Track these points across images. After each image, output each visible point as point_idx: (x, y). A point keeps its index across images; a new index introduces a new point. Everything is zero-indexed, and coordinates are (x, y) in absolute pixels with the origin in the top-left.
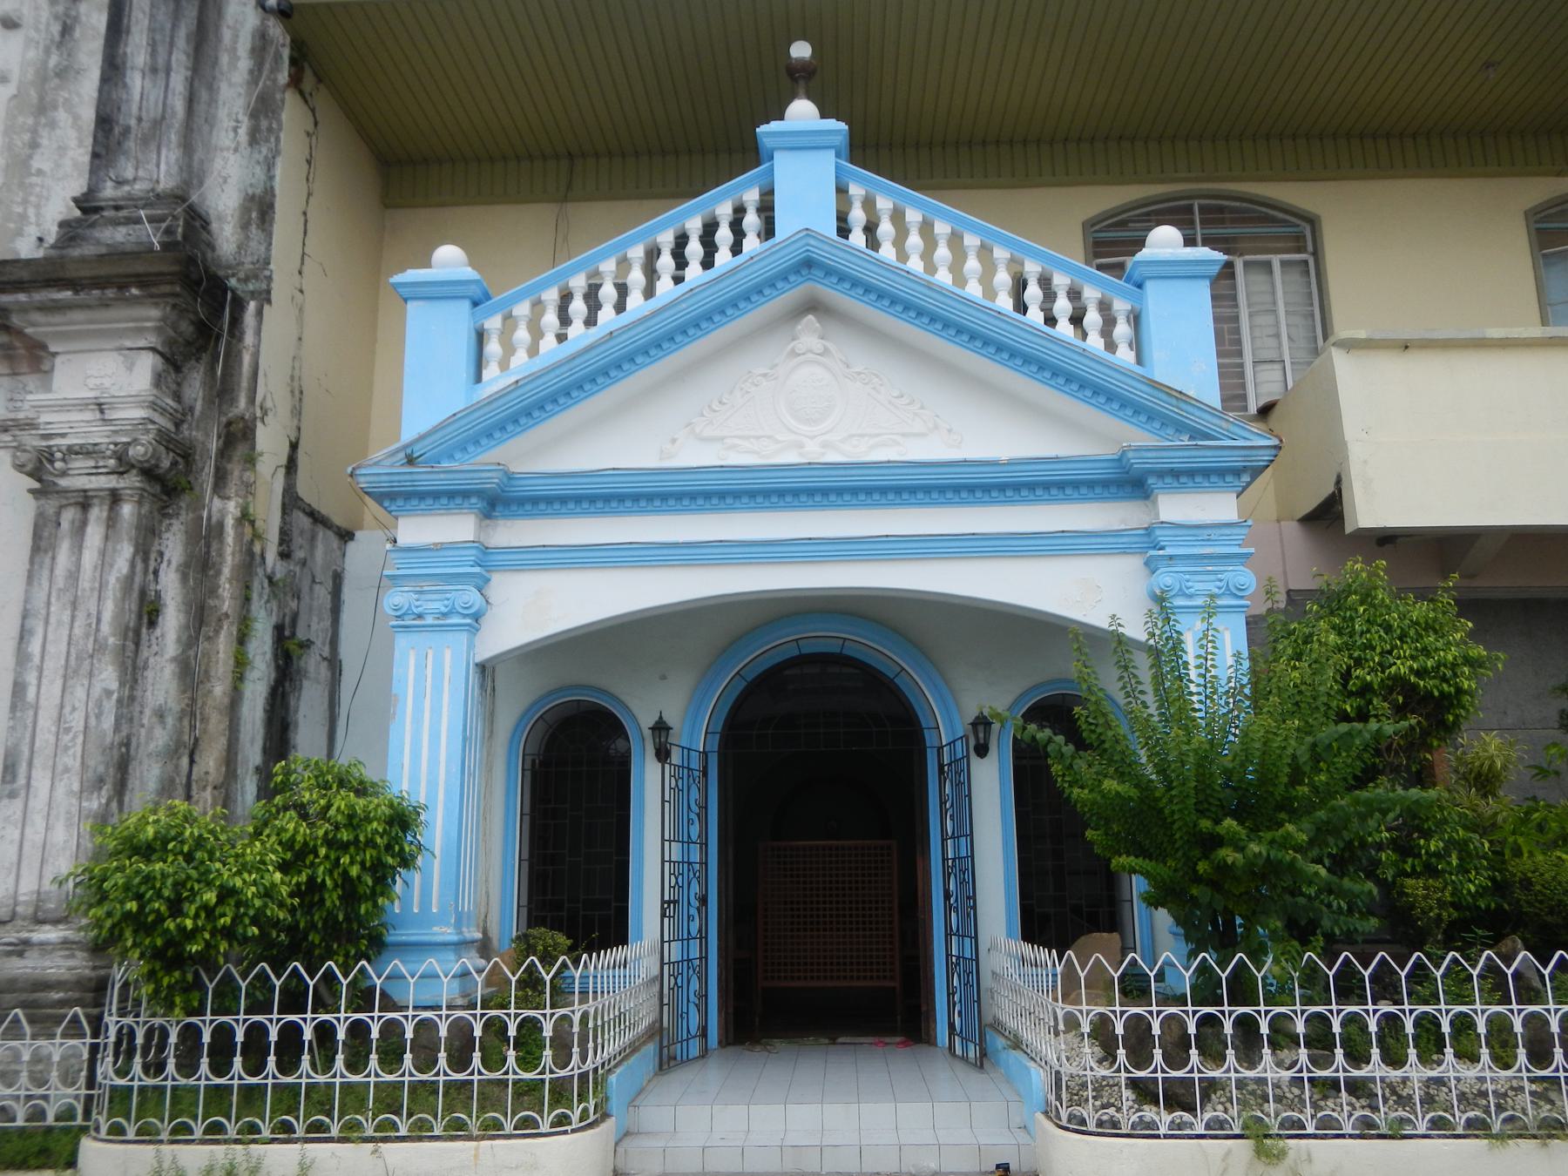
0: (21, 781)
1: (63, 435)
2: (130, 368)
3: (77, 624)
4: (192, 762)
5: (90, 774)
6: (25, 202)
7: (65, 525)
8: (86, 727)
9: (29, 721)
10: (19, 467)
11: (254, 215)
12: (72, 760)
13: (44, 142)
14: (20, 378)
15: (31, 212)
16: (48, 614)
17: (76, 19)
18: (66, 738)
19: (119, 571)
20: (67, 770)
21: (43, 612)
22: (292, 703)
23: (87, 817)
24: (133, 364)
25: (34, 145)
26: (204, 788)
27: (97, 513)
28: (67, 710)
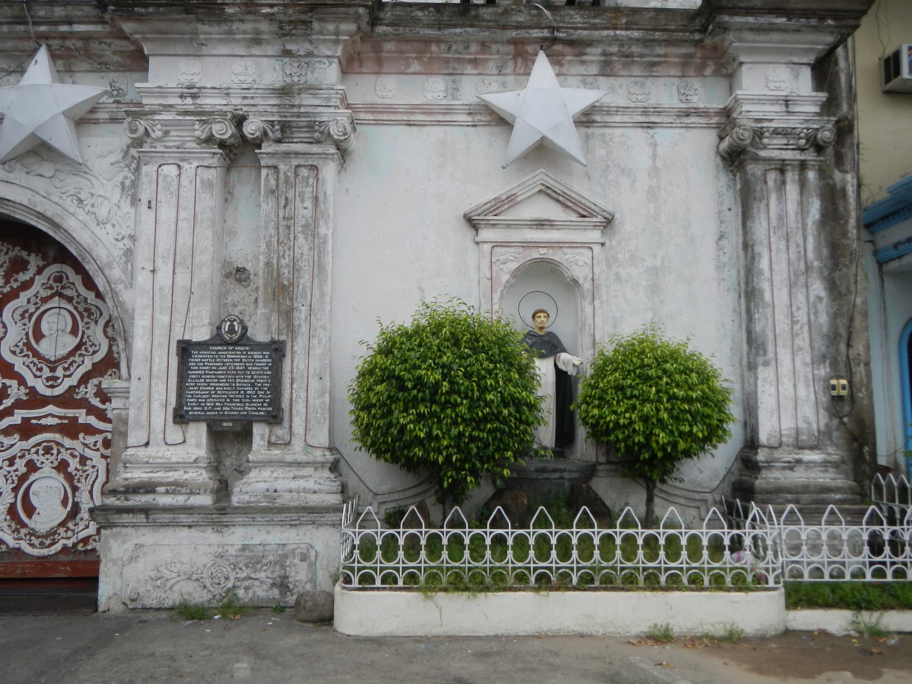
0: (771, 355)
3: (791, 251)
4: (849, 345)
5: (816, 352)
7: (771, 183)
8: (809, 321)
9: (769, 315)
12: (803, 341)
14: (685, 79)
16: (770, 243)
18: (796, 328)
19: (813, 216)
20: (800, 349)
21: (766, 242)
23: (819, 380)
26: (858, 364)
28: (794, 308)
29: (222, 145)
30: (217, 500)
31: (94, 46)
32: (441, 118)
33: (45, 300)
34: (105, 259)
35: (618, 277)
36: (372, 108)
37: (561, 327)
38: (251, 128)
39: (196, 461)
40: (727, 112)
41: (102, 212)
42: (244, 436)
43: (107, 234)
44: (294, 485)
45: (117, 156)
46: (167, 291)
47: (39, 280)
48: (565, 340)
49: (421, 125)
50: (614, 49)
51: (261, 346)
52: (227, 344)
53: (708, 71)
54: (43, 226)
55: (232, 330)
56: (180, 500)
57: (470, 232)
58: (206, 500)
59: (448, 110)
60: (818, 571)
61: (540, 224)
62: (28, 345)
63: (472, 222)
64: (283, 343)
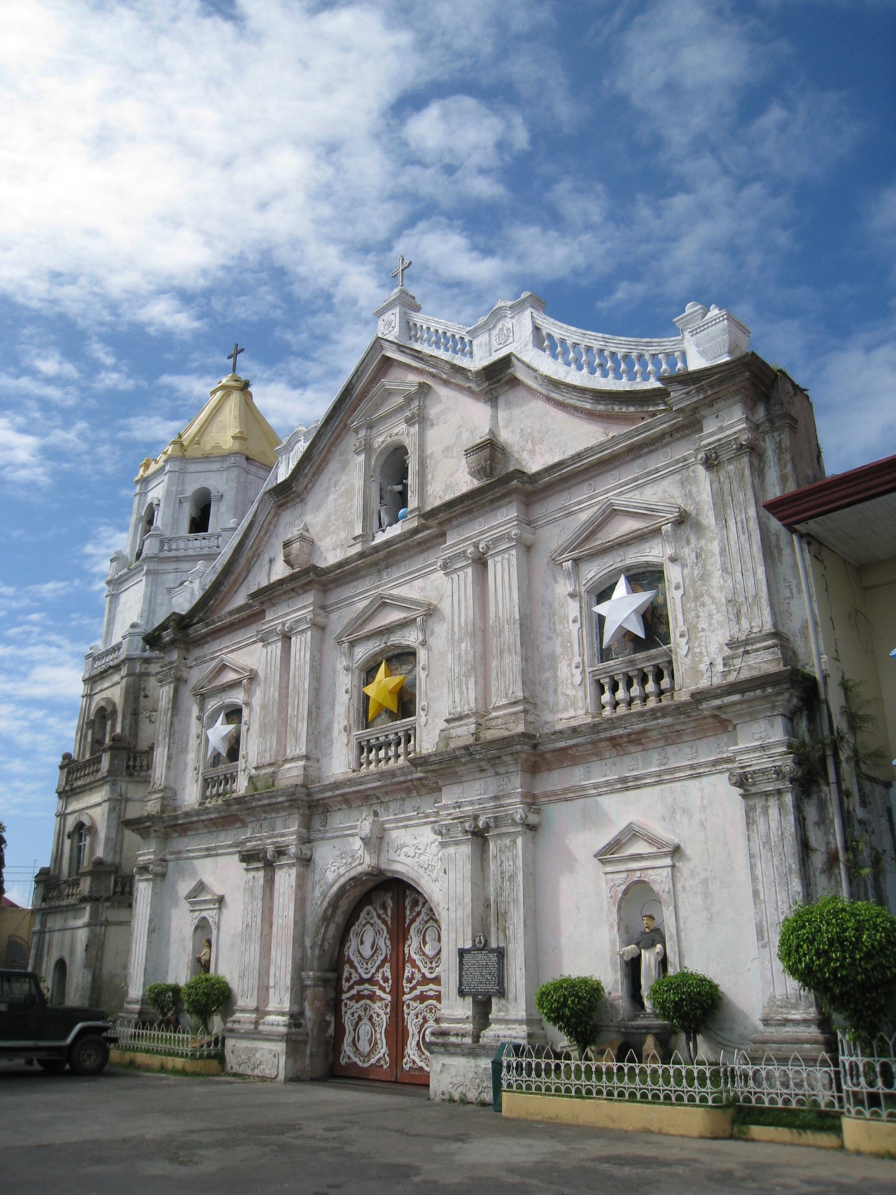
1: (750, 766)
2: (772, 726)
6: (700, 646)
10: (735, 784)
13: (701, 614)
15: (704, 650)
17: (701, 549)
22: (883, 885)
24: (773, 724)
25: (698, 617)
30: (474, 1042)
31: (424, 782)
32: (581, 793)
33: (426, 922)
35: (684, 888)
36: (546, 795)
39: (467, 1018)
44: (508, 1033)
46: (454, 920)
47: (424, 910)
50: (665, 730)
51: (492, 951)
52: (478, 950)
54: (413, 884)
55: (480, 942)
60: (786, 1102)
62: (420, 948)
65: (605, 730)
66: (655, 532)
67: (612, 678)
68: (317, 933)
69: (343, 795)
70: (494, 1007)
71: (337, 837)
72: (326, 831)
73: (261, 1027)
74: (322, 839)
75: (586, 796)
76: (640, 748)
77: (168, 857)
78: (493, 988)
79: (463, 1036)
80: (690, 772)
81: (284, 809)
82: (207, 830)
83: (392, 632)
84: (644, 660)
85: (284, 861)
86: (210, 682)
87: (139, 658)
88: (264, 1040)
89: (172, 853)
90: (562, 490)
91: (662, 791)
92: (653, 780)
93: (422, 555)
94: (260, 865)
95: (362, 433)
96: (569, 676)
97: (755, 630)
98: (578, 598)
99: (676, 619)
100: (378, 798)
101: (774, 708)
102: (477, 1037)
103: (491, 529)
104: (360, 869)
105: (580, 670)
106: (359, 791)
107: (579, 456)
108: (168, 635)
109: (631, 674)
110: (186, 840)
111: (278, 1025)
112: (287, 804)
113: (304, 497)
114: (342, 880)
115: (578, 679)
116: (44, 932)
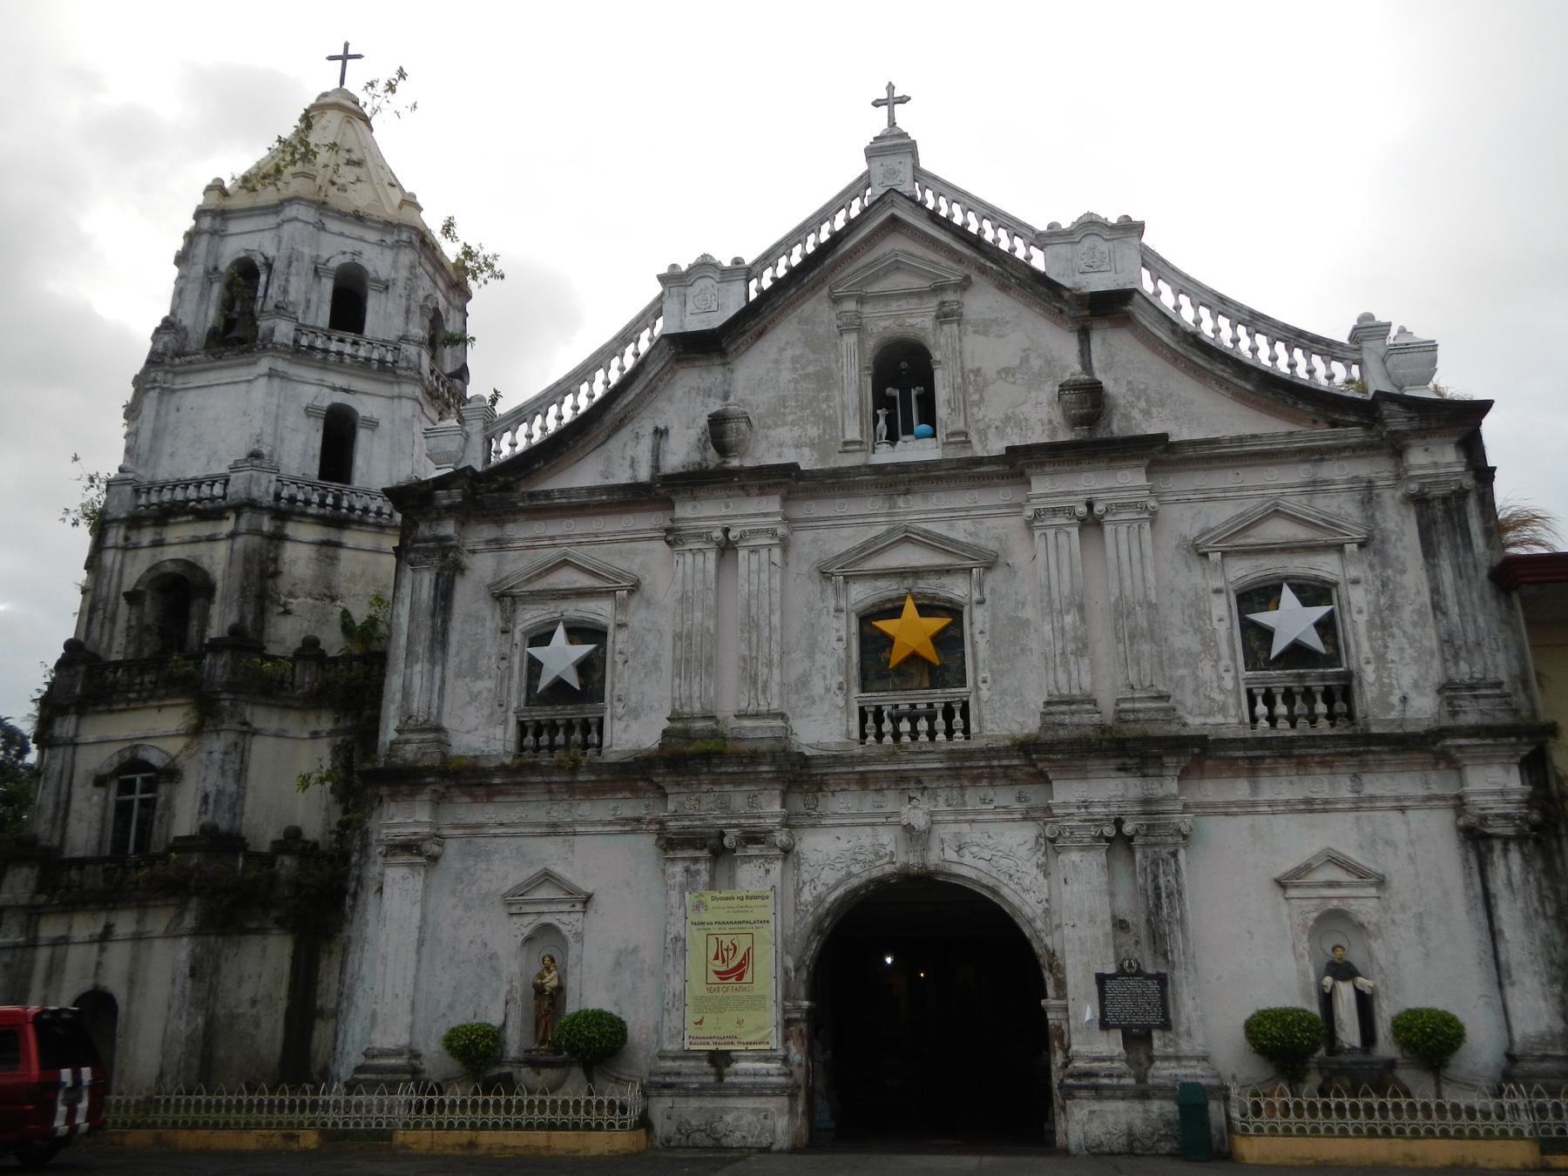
2: (1508, 772)
11: (1519, 686)
13: (1390, 644)
15: (1395, 682)
17: (1388, 577)
25: (1386, 647)
27: (1512, 846)
29: (1108, 839)
30: (1138, 1081)
31: (1010, 772)
34: (1031, 915)
35: (1393, 921)
37: (1356, 956)
38: (1128, 828)
40: (1459, 798)
41: (1027, 882)
42: (1146, 1038)
43: (1031, 898)
45: (1031, 843)
48: (1358, 965)
49: (1236, 814)
53: (1442, 766)
55: (1130, 965)
56: (1115, 1081)
57: (1279, 891)
58: (1130, 1081)
59: (1254, 804)
61: (1331, 884)
63: (1282, 884)
64: (1165, 975)
65: (1300, 747)
66: (1339, 548)
67: (1268, 690)
68: (807, 948)
69: (861, 773)
70: (1156, 1043)
71: (842, 825)
72: (821, 816)
73: (727, 1080)
74: (813, 826)
75: (1257, 813)
76: (1327, 771)
77: (446, 832)
78: (1153, 1018)
79: (1120, 1076)
80: (1394, 804)
81: (752, 782)
82: (547, 797)
83: (922, 578)
84: (1315, 678)
85: (753, 850)
86: (529, 581)
87: (269, 509)
88: (741, 1095)
89: (456, 826)
90: (1197, 470)
91: (1358, 819)
92: (1347, 806)
93: (969, 492)
94: (705, 853)
95: (850, 306)
96: (1215, 678)
97: (1477, 675)
98: (1224, 595)
99: (1357, 644)
100: (920, 782)
101: (1512, 757)
102: (1141, 1079)
103: (1109, 490)
104: (889, 869)
105: (1232, 673)
106: (895, 771)
107: (1241, 440)
108: (449, 497)
109: (1295, 690)
110: (490, 808)
111: (768, 1074)
112: (770, 776)
113: (729, 360)
114: (855, 882)
115: (1229, 683)
116: (33, 944)
